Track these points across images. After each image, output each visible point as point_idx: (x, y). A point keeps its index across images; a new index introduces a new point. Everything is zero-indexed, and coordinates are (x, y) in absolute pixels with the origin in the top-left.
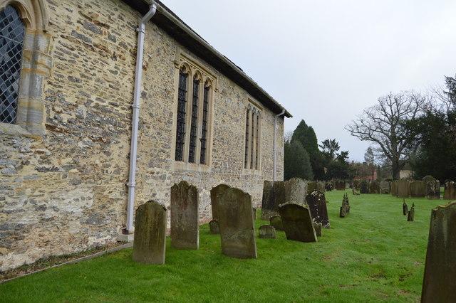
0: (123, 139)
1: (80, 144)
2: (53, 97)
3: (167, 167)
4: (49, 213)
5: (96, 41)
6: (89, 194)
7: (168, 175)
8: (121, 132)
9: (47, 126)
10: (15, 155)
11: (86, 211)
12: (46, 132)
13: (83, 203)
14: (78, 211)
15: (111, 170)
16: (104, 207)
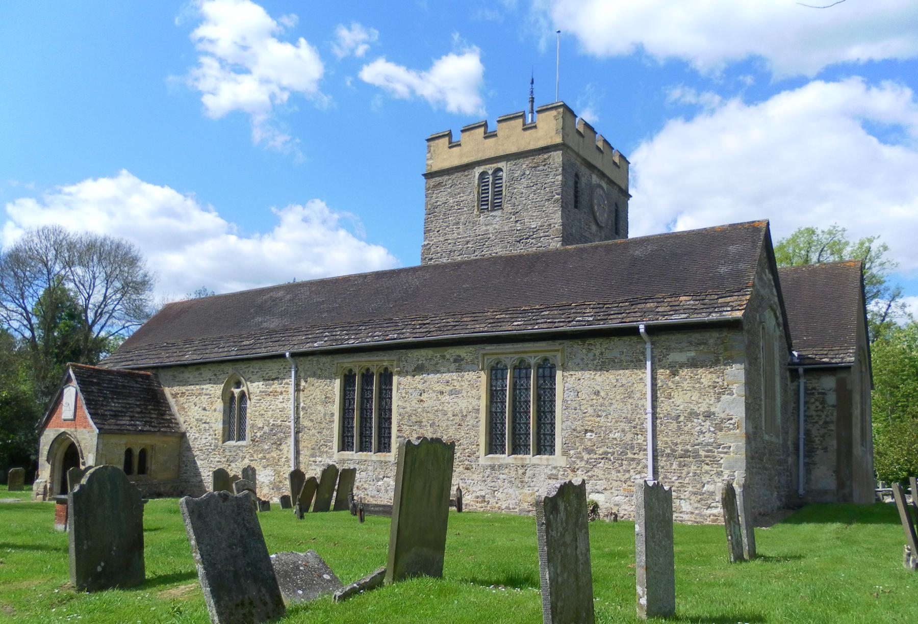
1: (266, 447)
5: (271, 390)
6: (272, 473)
10: (241, 454)
11: (271, 483)
13: (269, 478)
14: (267, 482)
15: (283, 460)
16: (280, 482)
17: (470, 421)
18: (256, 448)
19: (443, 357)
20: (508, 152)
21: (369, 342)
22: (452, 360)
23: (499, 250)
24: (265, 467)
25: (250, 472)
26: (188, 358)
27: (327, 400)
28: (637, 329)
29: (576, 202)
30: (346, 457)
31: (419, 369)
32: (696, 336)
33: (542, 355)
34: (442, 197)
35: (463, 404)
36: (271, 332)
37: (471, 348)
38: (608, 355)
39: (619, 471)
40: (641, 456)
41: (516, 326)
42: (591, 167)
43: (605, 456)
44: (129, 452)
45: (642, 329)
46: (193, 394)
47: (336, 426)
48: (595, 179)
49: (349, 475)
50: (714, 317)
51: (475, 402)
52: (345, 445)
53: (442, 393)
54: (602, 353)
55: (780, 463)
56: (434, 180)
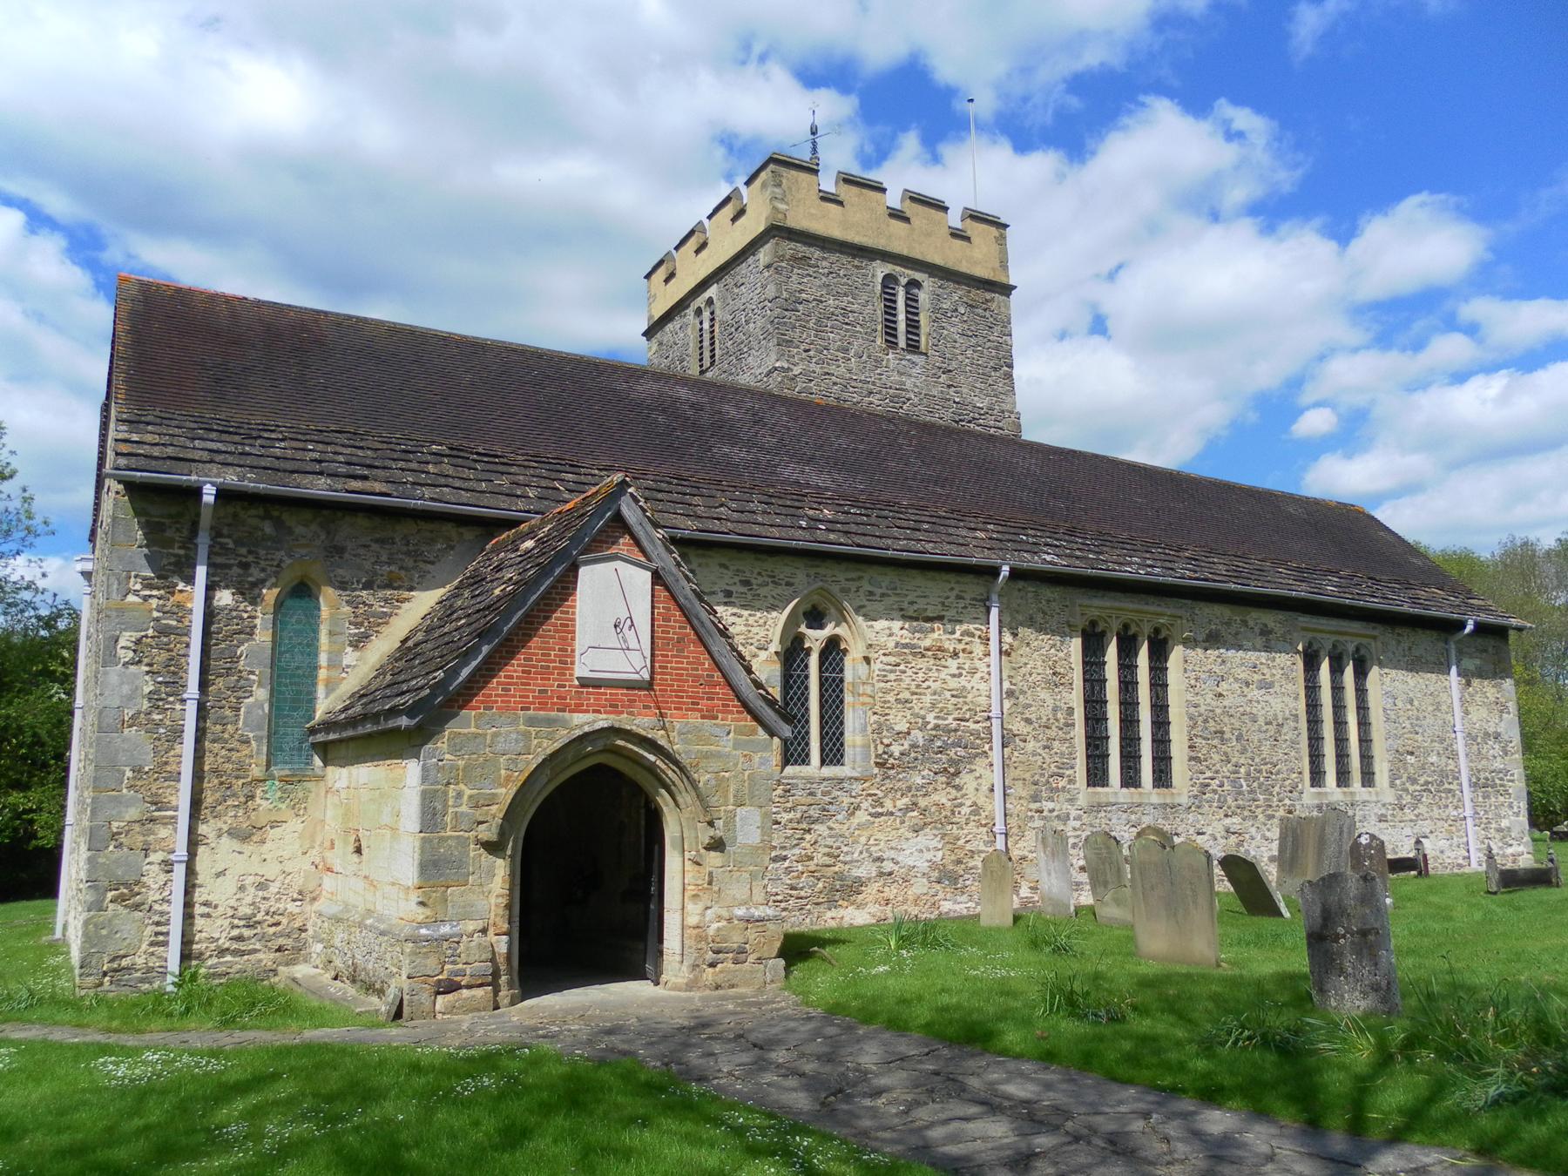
0: (980, 765)
1: (919, 781)
2: (878, 730)
3: (1071, 801)
4: (888, 866)
5: (927, 643)
6: (935, 843)
7: (1073, 813)
8: (977, 755)
9: (877, 764)
10: (847, 800)
11: (933, 866)
12: (876, 770)
13: (929, 856)
14: (923, 866)
15: (965, 810)
16: (959, 862)
18: (888, 784)
19: (1245, 623)
22: (1257, 630)
24: (916, 830)
27: (1057, 680)
30: (1104, 800)
31: (1213, 640)
33: (1357, 641)
37: (1281, 616)
47: (1079, 732)
53: (1248, 684)
56: (792, 245)
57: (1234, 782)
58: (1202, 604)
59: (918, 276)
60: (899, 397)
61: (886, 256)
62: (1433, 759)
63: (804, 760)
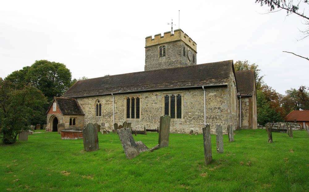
11: (108, 127)
16: (111, 126)
17: (160, 110)
20: (167, 42)
21: (133, 91)
23: (165, 67)
24: (106, 123)
25: (103, 124)
26: (85, 95)
27: (123, 106)
28: (202, 87)
29: (184, 54)
32: (216, 89)
34: (150, 53)
35: (157, 106)
36: (107, 89)
37: (160, 92)
38: (195, 94)
39: (197, 122)
40: (203, 118)
41: (171, 87)
42: (188, 46)
43: (194, 118)
44: (71, 120)
45: (203, 87)
46: (87, 104)
48: (189, 49)
49: (129, 124)
50: (221, 84)
51: (161, 106)
52: (128, 117)
54: (193, 93)
55: (236, 119)
57: (149, 118)
58: (145, 93)
59: (164, 45)
60: (160, 64)
61: (159, 44)
62: (197, 113)
63: (98, 116)
